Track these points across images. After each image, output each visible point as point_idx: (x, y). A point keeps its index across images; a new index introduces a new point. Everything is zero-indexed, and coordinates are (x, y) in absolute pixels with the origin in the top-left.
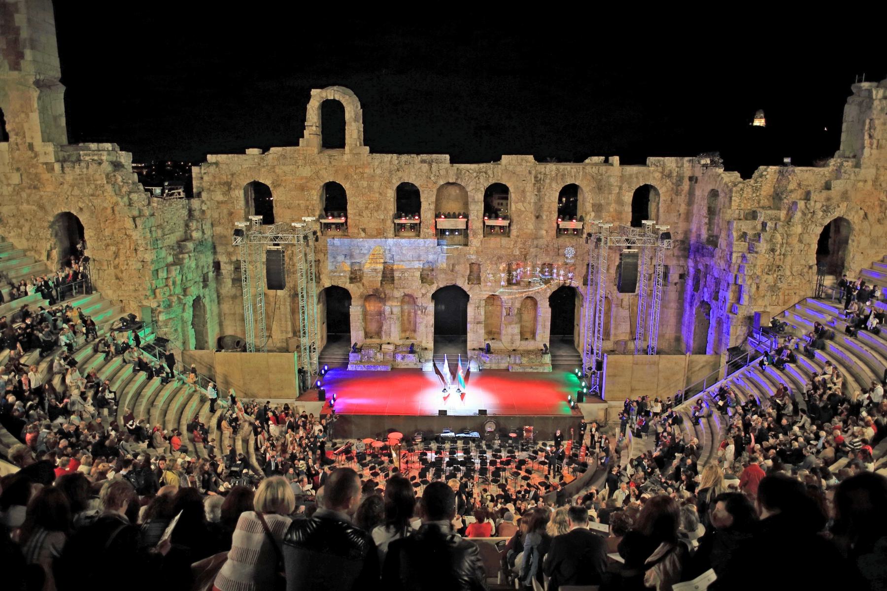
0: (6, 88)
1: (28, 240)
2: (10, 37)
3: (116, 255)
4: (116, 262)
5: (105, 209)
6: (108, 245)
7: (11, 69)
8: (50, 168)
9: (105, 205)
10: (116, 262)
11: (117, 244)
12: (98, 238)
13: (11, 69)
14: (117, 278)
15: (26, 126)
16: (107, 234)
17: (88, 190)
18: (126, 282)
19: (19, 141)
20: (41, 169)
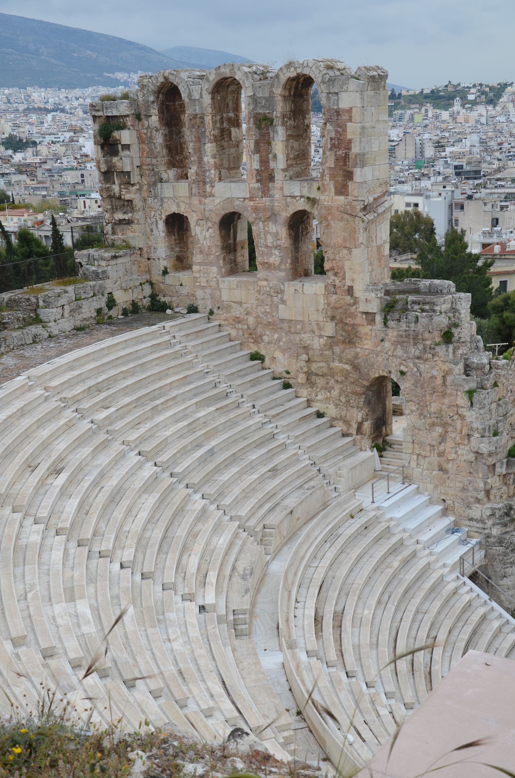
0: (329, 218)
1: (337, 406)
2: (340, 153)
3: (443, 438)
4: (442, 448)
5: (433, 377)
6: (433, 425)
7: (336, 194)
8: (370, 316)
9: (435, 373)
10: (442, 448)
11: (445, 425)
12: (421, 414)
13: (336, 194)
14: (441, 469)
15: (347, 265)
16: (432, 410)
17: (414, 351)
18: (451, 477)
19: (337, 283)
20: (360, 319)
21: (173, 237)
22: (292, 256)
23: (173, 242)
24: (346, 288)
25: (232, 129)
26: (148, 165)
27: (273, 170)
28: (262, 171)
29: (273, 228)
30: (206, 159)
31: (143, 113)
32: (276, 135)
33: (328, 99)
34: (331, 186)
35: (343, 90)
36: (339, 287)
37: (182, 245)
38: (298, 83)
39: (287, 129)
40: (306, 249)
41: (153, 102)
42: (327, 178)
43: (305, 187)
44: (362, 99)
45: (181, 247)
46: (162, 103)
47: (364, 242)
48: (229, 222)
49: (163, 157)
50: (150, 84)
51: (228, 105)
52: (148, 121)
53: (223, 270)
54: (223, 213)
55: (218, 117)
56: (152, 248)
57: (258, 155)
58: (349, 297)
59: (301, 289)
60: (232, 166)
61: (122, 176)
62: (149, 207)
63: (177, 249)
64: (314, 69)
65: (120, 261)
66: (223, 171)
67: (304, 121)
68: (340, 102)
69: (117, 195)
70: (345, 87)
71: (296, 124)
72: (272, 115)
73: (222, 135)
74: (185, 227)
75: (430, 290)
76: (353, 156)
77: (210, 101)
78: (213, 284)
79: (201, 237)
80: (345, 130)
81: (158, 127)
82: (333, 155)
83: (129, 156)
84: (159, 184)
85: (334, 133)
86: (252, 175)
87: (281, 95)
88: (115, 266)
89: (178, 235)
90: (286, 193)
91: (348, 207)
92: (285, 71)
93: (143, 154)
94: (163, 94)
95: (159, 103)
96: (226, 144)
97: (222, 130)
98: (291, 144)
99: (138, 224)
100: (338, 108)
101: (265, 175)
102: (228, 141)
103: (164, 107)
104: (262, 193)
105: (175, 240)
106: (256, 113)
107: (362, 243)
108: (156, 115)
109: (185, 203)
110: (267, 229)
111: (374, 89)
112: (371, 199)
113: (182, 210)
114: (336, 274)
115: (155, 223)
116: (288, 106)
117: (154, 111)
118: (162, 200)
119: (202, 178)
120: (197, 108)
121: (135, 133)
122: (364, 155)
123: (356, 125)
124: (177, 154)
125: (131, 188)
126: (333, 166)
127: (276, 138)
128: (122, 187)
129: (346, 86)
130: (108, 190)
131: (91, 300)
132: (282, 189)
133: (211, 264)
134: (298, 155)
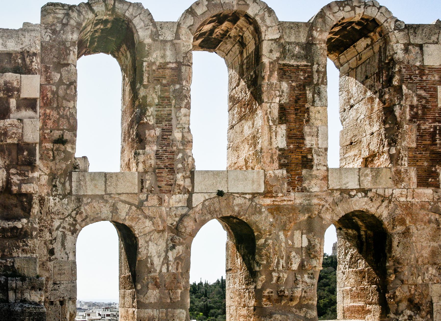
0: (407, 222)
2: (426, 126)
27: (310, 150)
28: (291, 151)
32: (317, 98)
33: (406, 50)
34: (413, 174)
42: (405, 162)
43: (367, 175)
57: (284, 127)
62: (49, 213)
68: (425, 57)
70: (434, 38)
72: (312, 69)
80: (434, 96)
82: (415, 130)
85: (415, 99)
86: (272, 157)
93: (45, 124)
100: (423, 66)
101: (296, 157)
104: (289, 184)
106: (284, 65)
109: (129, 203)
115: (59, 239)
118: (79, 199)
126: (414, 145)
132: (326, 178)
133: (174, 305)
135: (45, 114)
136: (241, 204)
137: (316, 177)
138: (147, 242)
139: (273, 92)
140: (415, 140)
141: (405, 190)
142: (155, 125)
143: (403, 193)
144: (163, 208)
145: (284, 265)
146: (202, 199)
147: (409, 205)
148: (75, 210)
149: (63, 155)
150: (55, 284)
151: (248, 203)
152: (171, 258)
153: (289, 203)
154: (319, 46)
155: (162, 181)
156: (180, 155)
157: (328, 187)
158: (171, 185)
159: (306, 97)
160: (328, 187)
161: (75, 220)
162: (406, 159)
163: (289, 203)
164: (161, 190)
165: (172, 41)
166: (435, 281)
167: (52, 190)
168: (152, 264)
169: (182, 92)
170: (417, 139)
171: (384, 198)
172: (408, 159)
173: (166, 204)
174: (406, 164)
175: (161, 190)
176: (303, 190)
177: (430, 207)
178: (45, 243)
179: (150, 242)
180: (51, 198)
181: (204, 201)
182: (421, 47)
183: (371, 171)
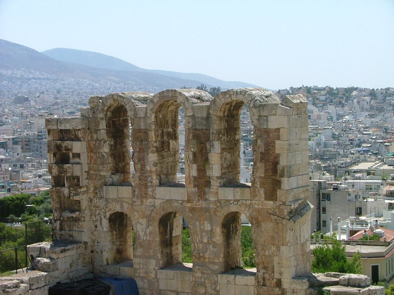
15: (276, 259)
19: (266, 276)
21: (115, 232)
22: (225, 251)
23: (114, 237)
24: (275, 280)
25: (171, 141)
26: (95, 171)
29: (208, 227)
30: (148, 168)
31: (93, 126)
32: (212, 149)
33: (258, 120)
34: (262, 192)
35: (272, 114)
36: (269, 280)
37: (122, 239)
38: (231, 106)
39: (221, 144)
40: (236, 245)
41: (102, 119)
43: (238, 192)
44: (289, 121)
45: (121, 241)
46: (110, 118)
47: (291, 241)
48: (166, 221)
49: (109, 164)
50: (100, 104)
51: (167, 121)
52: (97, 134)
53: (161, 262)
54: (163, 213)
55: (160, 132)
56: (96, 242)
58: (277, 289)
59: (234, 281)
60: (170, 172)
61: (72, 180)
63: (118, 243)
64: (246, 96)
65: (68, 254)
66: (163, 177)
67: (235, 136)
68: (269, 123)
69: (66, 195)
70: (274, 112)
71: (228, 140)
73: (163, 147)
74: (125, 222)
75: (348, 282)
76: (281, 168)
77: (153, 120)
78: (153, 275)
79: (142, 234)
80: (274, 147)
81: (106, 139)
82: (263, 166)
83: (79, 163)
84: (105, 187)
87: (217, 116)
88: (63, 259)
89: (119, 230)
90: (221, 197)
91: (277, 210)
92: (221, 97)
93: (91, 161)
94: (110, 112)
95: (107, 119)
96: (165, 154)
97: (163, 143)
98: (224, 156)
99: (84, 221)
102: (167, 152)
103: (111, 122)
105: (116, 235)
107: (289, 242)
108: (104, 129)
110: (202, 227)
111: (297, 114)
112: (297, 205)
113: (126, 209)
114: (265, 268)
115: (99, 220)
116: (223, 125)
117: (103, 125)
119: (144, 182)
120: (142, 124)
121: (84, 143)
122: (290, 167)
123: (283, 142)
124: (119, 162)
125: (79, 190)
126: (263, 176)
127: (212, 151)
128: (72, 189)
129: (275, 110)
130: (58, 192)
131: (42, 289)
132: (217, 193)
133: (149, 257)
134: (230, 164)
135: (91, 156)
136: (176, 206)
137: (212, 192)
138: (136, 224)
139: (190, 146)
140: (263, 172)
141: (258, 201)
142: (138, 162)
143: (257, 203)
144: (143, 206)
145: (200, 239)
146: (160, 202)
147: (260, 210)
148: (105, 205)
149: (99, 177)
150: (98, 242)
151: (180, 205)
152: (147, 233)
153: (199, 206)
154: (213, 118)
155: (142, 192)
156: (150, 179)
157: (218, 198)
158: (146, 194)
159: (206, 148)
160: (218, 198)
161: (105, 211)
162: (259, 183)
163: (199, 206)
164: (142, 197)
165: (143, 117)
166: (275, 255)
167: (95, 195)
168: (139, 235)
169: (148, 145)
170: (265, 172)
171: (246, 206)
172: (260, 184)
173: (144, 204)
174: (259, 187)
175: (142, 197)
176: (206, 200)
177: (272, 211)
178: (93, 222)
179: (138, 224)
180: (95, 199)
181: (161, 203)
182: (267, 117)
183: (240, 190)
